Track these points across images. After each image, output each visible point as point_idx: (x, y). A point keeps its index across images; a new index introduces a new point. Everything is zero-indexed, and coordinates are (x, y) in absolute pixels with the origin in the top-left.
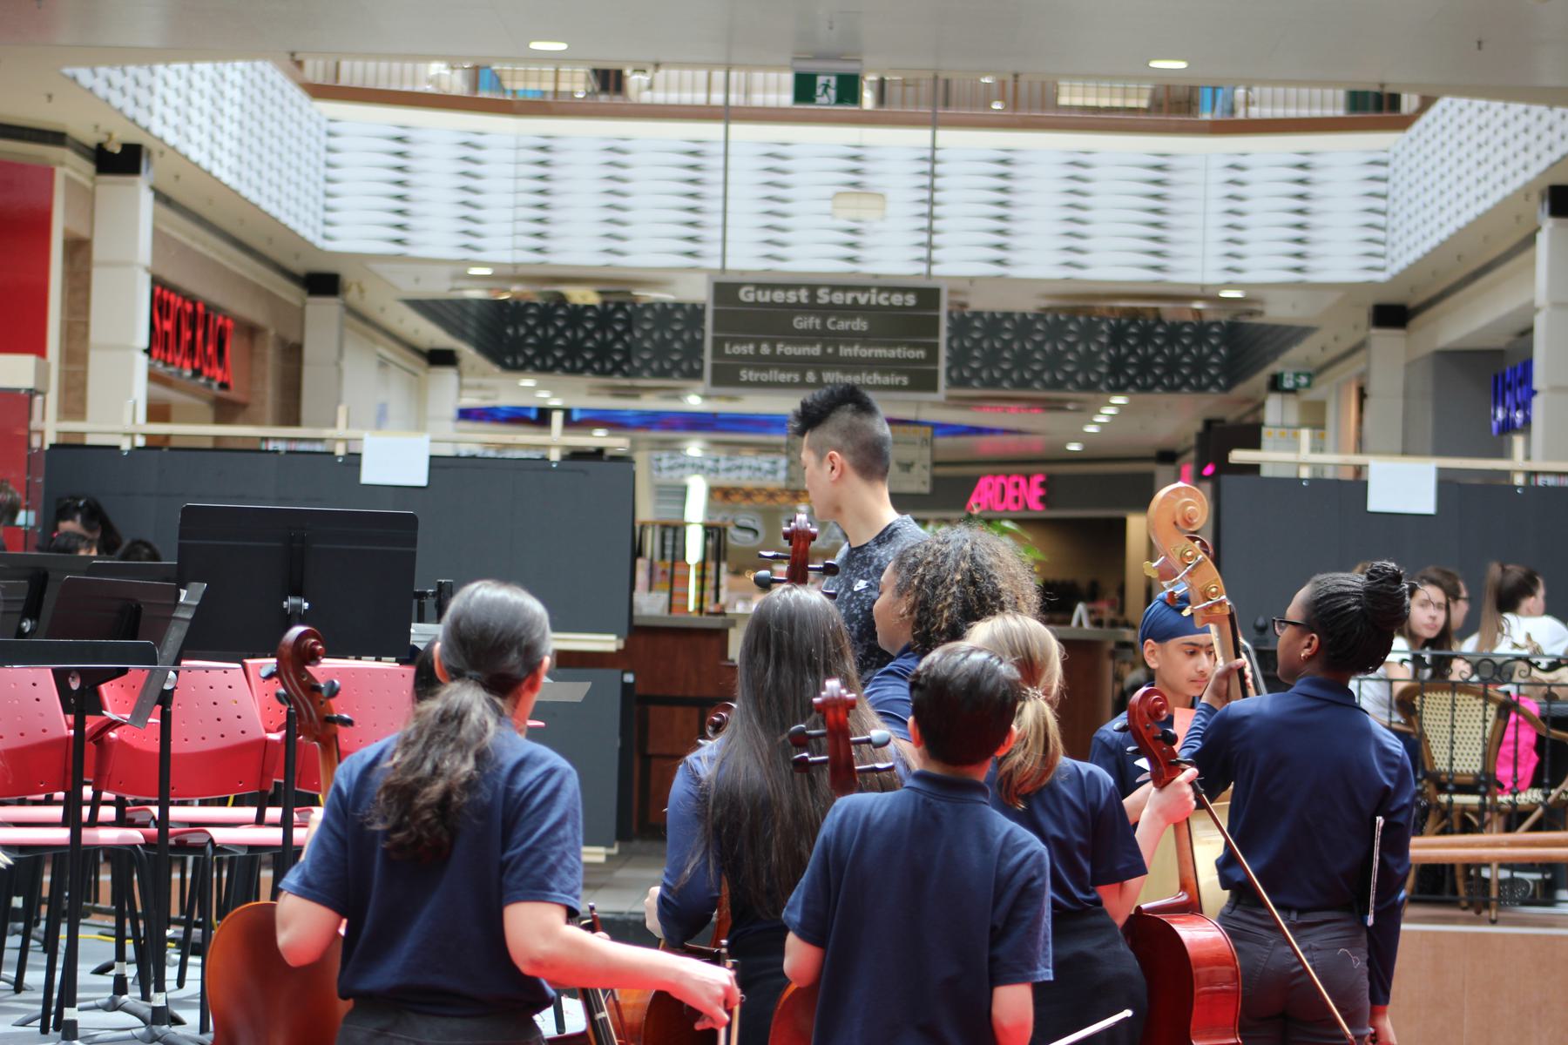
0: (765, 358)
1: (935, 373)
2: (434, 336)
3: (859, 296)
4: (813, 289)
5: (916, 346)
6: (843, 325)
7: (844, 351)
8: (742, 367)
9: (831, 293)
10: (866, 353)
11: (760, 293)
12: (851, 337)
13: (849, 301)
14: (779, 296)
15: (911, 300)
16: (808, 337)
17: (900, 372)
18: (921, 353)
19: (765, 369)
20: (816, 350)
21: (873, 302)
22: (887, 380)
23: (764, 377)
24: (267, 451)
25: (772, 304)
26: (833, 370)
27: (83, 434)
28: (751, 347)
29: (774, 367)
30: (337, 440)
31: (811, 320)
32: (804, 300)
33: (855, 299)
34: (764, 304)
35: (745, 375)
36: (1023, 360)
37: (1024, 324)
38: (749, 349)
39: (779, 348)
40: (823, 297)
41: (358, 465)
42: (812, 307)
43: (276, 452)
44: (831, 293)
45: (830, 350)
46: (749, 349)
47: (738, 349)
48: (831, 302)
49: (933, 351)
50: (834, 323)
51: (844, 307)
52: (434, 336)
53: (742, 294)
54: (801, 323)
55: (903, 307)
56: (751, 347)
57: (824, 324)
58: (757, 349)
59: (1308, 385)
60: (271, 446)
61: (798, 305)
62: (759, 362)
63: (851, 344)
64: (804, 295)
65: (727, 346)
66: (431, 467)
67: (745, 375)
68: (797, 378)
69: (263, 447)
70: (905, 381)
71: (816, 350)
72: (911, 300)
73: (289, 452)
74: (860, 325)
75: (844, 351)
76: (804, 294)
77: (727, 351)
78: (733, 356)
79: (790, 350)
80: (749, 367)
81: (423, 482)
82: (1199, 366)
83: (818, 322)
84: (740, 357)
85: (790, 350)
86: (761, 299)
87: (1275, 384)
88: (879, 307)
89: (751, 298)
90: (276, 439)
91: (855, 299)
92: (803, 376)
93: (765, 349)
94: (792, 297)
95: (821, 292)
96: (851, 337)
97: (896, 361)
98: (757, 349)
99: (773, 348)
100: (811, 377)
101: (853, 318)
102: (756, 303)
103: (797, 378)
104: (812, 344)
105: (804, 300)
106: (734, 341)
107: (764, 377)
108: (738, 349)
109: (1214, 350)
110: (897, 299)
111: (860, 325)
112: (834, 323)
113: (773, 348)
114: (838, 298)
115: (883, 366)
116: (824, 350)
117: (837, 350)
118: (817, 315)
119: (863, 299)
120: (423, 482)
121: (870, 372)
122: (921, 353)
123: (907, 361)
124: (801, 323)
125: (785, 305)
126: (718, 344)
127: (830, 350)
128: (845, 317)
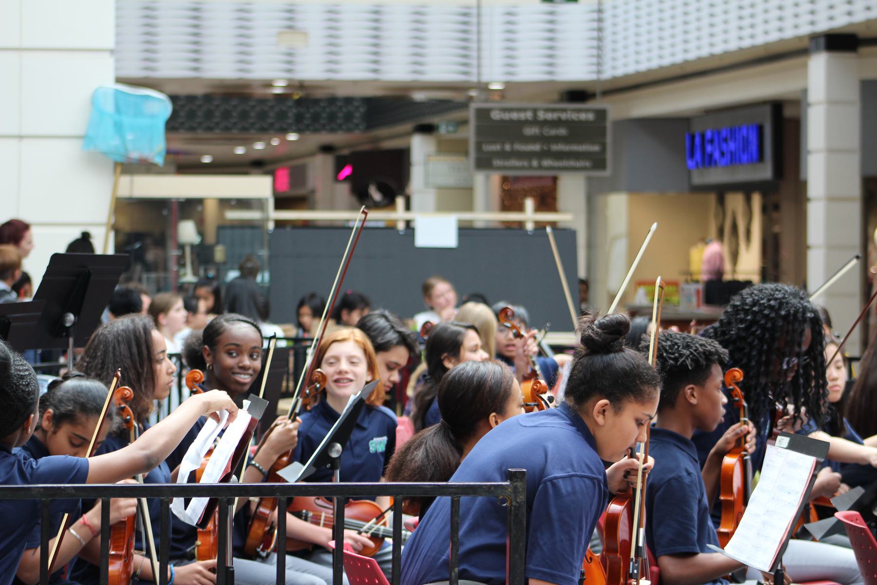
4: (535, 111)
6: (553, 132)
7: (555, 147)
12: (557, 139)
14: (515, 116)
16: (533, 139)
18: (596, 148)
20: (536, 147)
25: (511, 121)
36: (209, 115)
38: (496, 147)
40: (541, 115)
42: (535, 122)
45: (545, 148)
46: (496, 147)
49: (604, 146)
54: (530, 131)
55: (587, 122)
59: (454, 132)
64: (529, 115)
71: (536, 147)
74: (562, 132)
75: (555, 147)
82: (349, 117)
87: (427, 129)
88: (573, 122)
93: (508, 147)
94: (522, 116)
96: (557, 139)
102: (502, 121)
103: (525, 163)
110: (583, 116)
111: (562, 132)
114: (550, 116)
119: (564, 116)
122: (596, 148)
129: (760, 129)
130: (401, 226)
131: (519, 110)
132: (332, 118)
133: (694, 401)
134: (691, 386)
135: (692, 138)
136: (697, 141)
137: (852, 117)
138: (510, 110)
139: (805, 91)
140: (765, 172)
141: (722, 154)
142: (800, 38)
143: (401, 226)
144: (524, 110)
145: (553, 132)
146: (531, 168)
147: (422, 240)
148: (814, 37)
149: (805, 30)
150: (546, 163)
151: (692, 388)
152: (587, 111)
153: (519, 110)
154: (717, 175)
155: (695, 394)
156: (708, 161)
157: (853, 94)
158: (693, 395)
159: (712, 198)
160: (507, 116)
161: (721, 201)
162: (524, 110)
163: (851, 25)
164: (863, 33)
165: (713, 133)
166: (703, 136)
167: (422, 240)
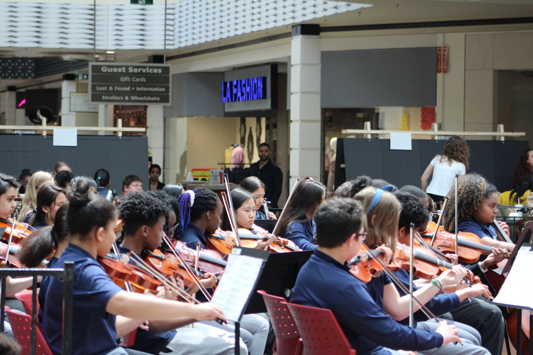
0: (111, 91)
1: (168, 96)
3: (143, 69)
4: (127, 67)
5: (162, 87)
6: (138, 80)
7: (138, 89)
8: (103, 95)
9: (133, 69)
10: (145, 89)
11: (109, 69)
12: (140, 84)
13: (139, 71)
14: (115, 70)
15: (160, 71)
16: (126, 84)
17: (157, 96)
18: (164, 89)
19: (111, 95)
20: (128, 89)
21: (148, 72)
22: (153, 99)
23: (111, 98)
24: (14, 134)
25: (113, 72)
26: (134, 95)
28: (106, 88)
29: (114, 95)
30: (43, 130)
31: (127, 78)
32: (124, 71)
33: (141, 71)
34: (105, 73)
35: (104, 97)
37: (15, 59)
38: (105, 88)
39: (116, 88)
40: (131, 70)
41: (52, 139)
42: (127, 74)
43: (18, 134)
44: (133, 69)
46: (105, 88)
47: (101, 89)
48: (133, 72)
49: (167, 88)
50: (134, 79)
51: (138, 73)
53: (102, 69)
54: (123, 79)
55: (158, 74)
56: (106, 88)
57: (131, 80)
58: (108, 88)
60: (16, 132)
61: (122, 73)
62: (108, 93)
63: (140, 86)
65: (97, 87)
66: (78, 139)
67: (104, 97)
68: (122, 98)
69: (13, 133)
70: (159, 99)
71: (128, 89)
72: (160, 71)
73: (23, 134)
74: (143, 80)
75: (138, 89)
76: (124, 69)
77: (97, 89)
78: (99, 91)
79: (119, 89)
80: (105, 95)
82: (24, 70)
83: (129, 79)
84: (102, 91)
85: (119, 89)
86: (109, 71)
87: (71, 78)
89: (106, 71)
90: (17, 130)
91: (141, 71)
92: (124, 98)
93: (111, 88)
94: (120, 70)
95: (130, 68)
96: (140, 84)
97: (155, 92)
98: (108, 88)
100: (127, 98)
101: (141, 77)
102: (107, 72)
104: (127, 87)
105: (124, 71)
106: (100, 86)
107: (111, 98)
108: (101, 89)
109: (30, 64)
110: (155, 71)
111: (143, 80)
114: (136, 70)
115: (151, 94)
117: (135, 89)
118: (129, 77)
121: (147, 96)
122: (164, 89)
123: (159, 92)
124: (123, 79)
125: (117, 73)
126: (94, 87)
127: (133, 89)
128: (138, 77)
129: (264, 79)
130: (45, 134)
131: (118, 67)
132: (14, 70)
133: (145, 235)
134: (145, 226)
135: (225, 84)
136: (228, 86)
137: (316, 73)
138: (113, 67)
139: (290, 57)
140: (266, 105)
141: (242, 94)
142: (287, 26)
143: (45, 134)
144: (121, 67)
145: (138, 80)
146: (124, 101)
147: (57, 142)
148: (294, 26)
149: (290, 22)
150: (133, 98)
151: (146, 228)
152: (158, 68)
153: (118, 67)
154: (239, 106)
155: (147, 231)
156: (234, 98)
157: (317, 60)
158: (145, 231)
159: (238, 119)
160: (110, 70)
161: (243, 122)
162: (121, 67)
163: (315, 18)
164: (323, 24)
165: (237, 81)
166: (231, 83)
167: (57, 142)
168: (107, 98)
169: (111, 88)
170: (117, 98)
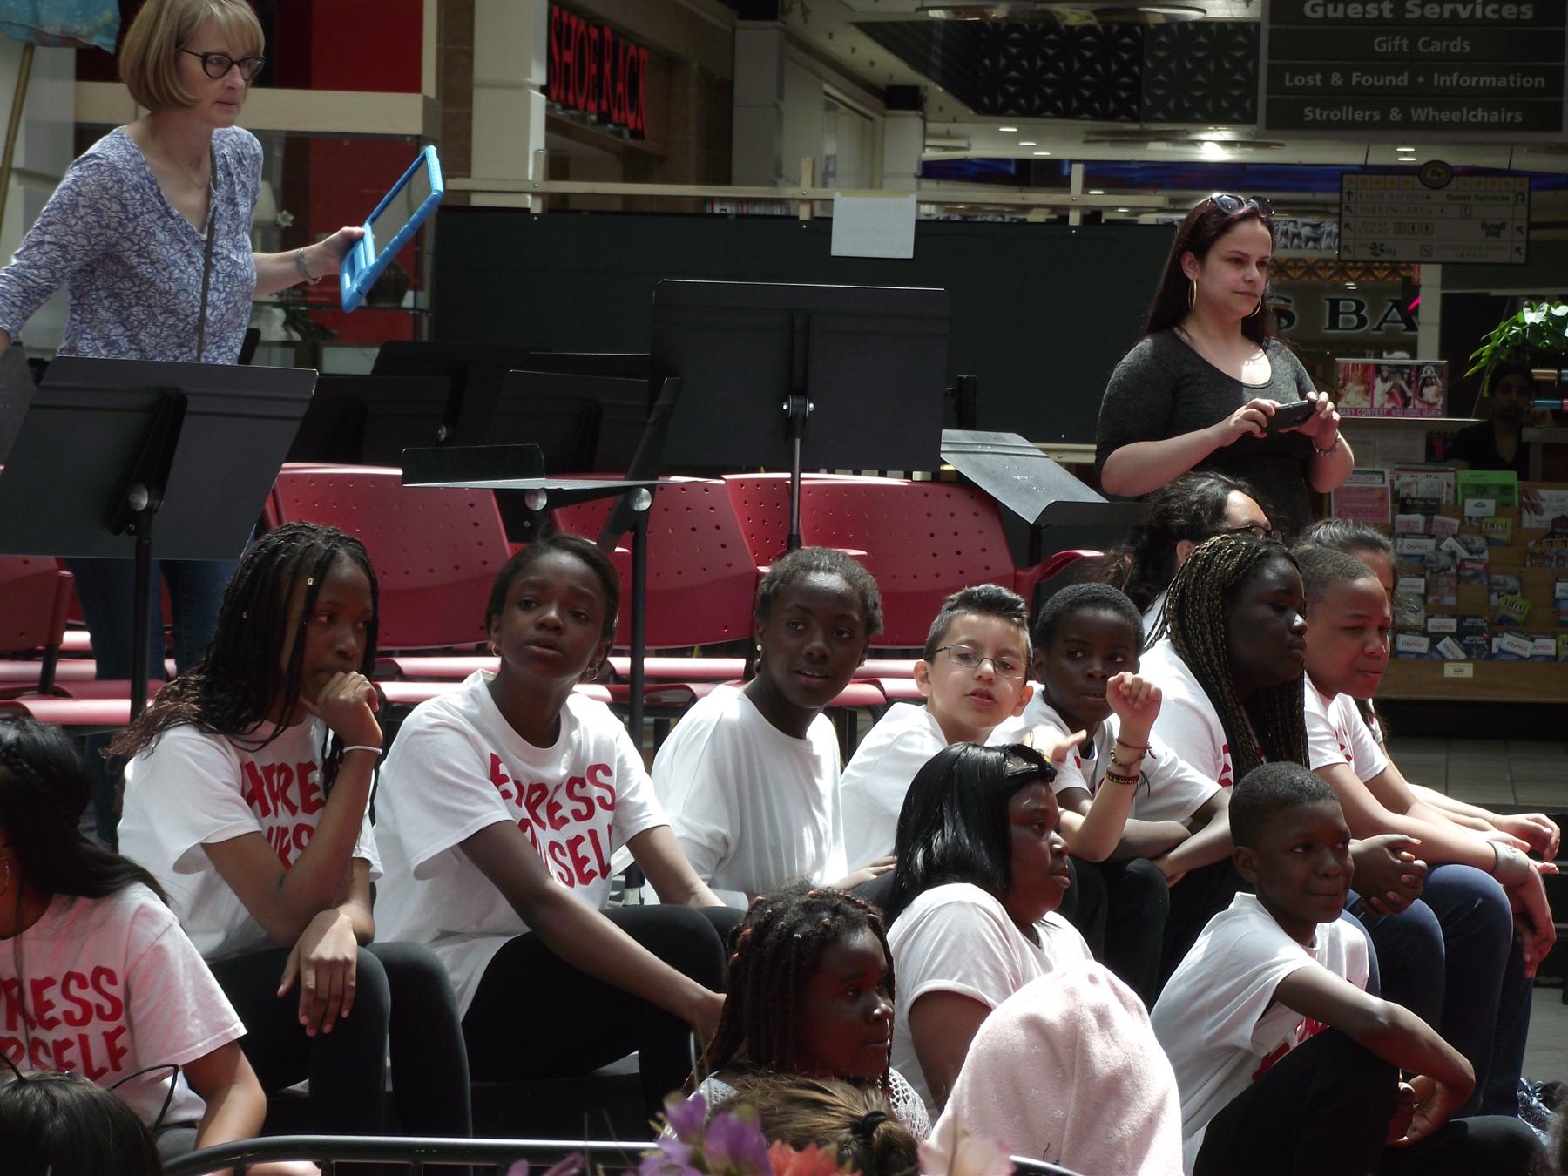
2: (890, 66)
6: (1438, 47)
7: (1439, 80)
10: (1466, 81)
13: (1446, 15)
18: (1540, 81)
20: (1403, 80)
23: (1335, 115)
24: (713, 215)
25: (1347, 20)
27: (468, 192)
32: (1387, 14)
33: (1454, 12)
34: (1336, 21)
39: (1355, 78)
43: (725, 216)
47: (1300, 81)
50: (1426, 44)
51: (1440, 22)
52: (890, 66)
54: (1381, 45)
57: (1412, 45)
58: (1326, 79)
68: (1377, 116)
71: (1403, 80)
73: (739, 216)
74: (1460, 46)
75: (1439, 80)
81: (910, 255)
85: (1367, 81)
90: (723, 200)
91: (1454, 12)
92: (1385, 115)
93: (1336, 80)
98: (1326, 79)
99: (1347, 77)
100: (1395, 115)
105: (1387, 14)
107: (1335, 115)
108: (1300, 81)
111: (1460, 46)
112: (1427, 45)
113: (1347, 77)
116: (1412, 79)
120: (910, 255)
122: (1540, 81)
124: (1381, 45)
125: (1363, 21)
126: (1275, 74)
145: (1438, 47)
147: (843, 244)
167: (843, 244)
168: (1319, 114)
169: (1336, 80)
170: (1358, 115)
